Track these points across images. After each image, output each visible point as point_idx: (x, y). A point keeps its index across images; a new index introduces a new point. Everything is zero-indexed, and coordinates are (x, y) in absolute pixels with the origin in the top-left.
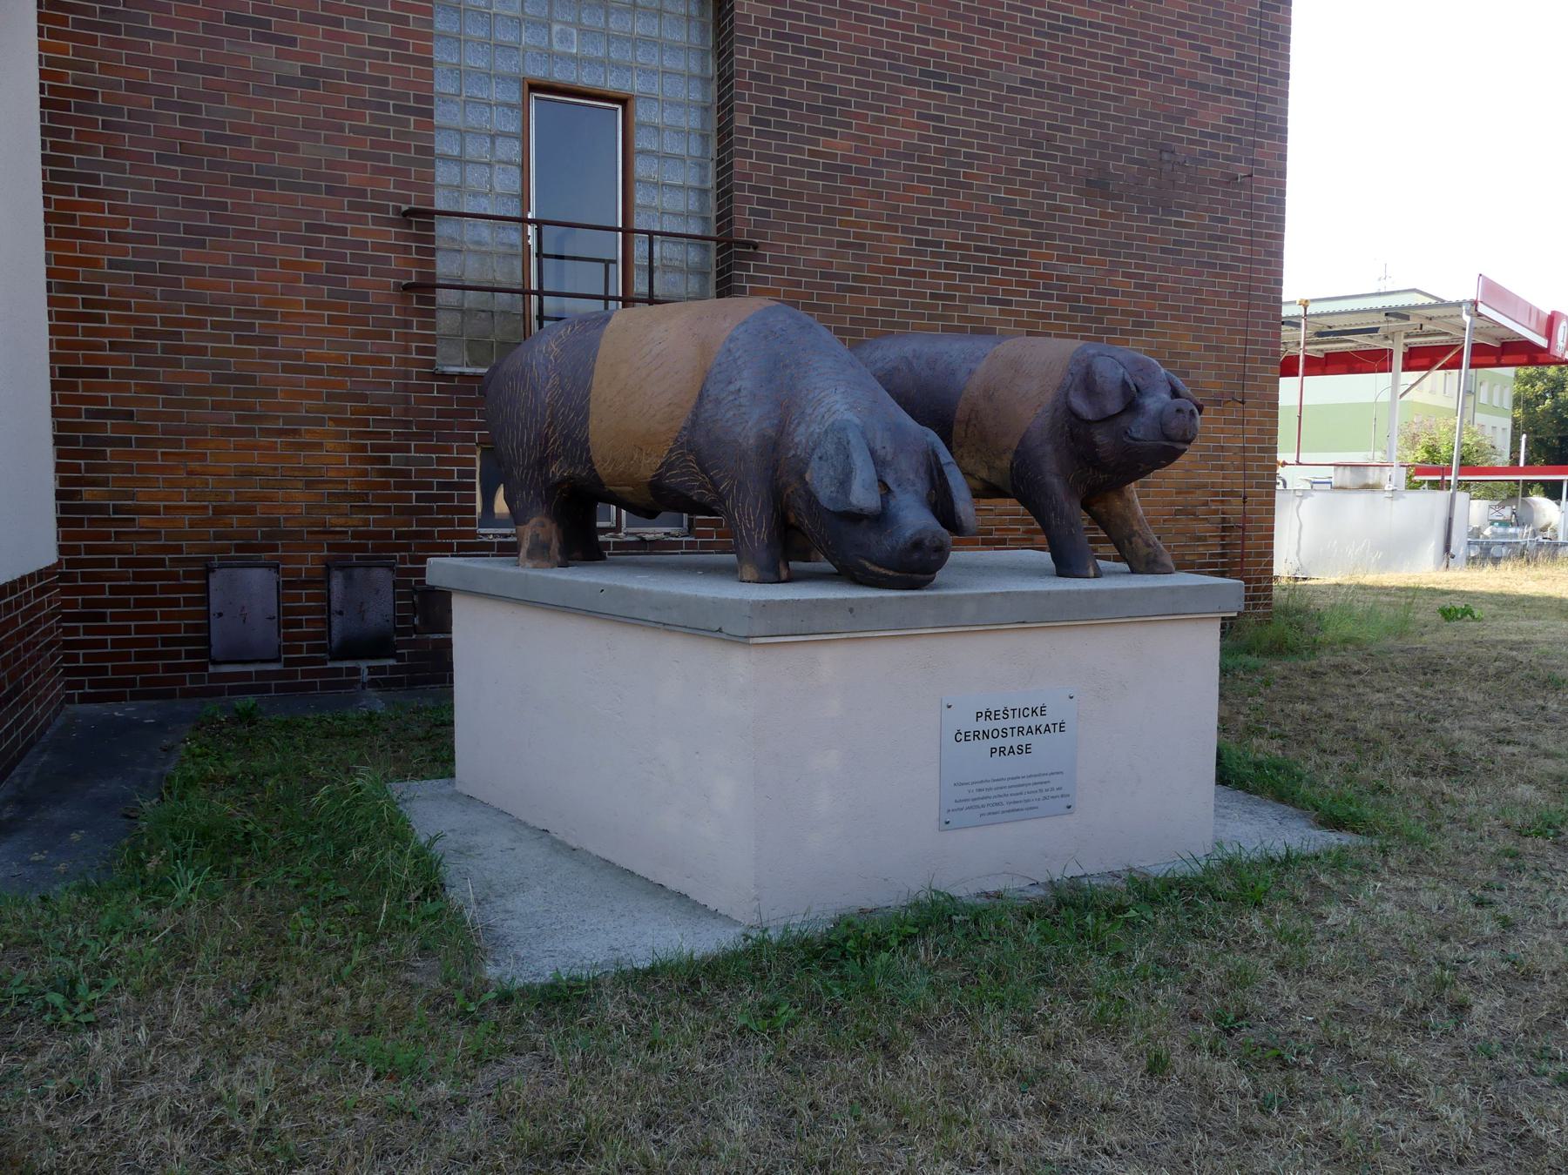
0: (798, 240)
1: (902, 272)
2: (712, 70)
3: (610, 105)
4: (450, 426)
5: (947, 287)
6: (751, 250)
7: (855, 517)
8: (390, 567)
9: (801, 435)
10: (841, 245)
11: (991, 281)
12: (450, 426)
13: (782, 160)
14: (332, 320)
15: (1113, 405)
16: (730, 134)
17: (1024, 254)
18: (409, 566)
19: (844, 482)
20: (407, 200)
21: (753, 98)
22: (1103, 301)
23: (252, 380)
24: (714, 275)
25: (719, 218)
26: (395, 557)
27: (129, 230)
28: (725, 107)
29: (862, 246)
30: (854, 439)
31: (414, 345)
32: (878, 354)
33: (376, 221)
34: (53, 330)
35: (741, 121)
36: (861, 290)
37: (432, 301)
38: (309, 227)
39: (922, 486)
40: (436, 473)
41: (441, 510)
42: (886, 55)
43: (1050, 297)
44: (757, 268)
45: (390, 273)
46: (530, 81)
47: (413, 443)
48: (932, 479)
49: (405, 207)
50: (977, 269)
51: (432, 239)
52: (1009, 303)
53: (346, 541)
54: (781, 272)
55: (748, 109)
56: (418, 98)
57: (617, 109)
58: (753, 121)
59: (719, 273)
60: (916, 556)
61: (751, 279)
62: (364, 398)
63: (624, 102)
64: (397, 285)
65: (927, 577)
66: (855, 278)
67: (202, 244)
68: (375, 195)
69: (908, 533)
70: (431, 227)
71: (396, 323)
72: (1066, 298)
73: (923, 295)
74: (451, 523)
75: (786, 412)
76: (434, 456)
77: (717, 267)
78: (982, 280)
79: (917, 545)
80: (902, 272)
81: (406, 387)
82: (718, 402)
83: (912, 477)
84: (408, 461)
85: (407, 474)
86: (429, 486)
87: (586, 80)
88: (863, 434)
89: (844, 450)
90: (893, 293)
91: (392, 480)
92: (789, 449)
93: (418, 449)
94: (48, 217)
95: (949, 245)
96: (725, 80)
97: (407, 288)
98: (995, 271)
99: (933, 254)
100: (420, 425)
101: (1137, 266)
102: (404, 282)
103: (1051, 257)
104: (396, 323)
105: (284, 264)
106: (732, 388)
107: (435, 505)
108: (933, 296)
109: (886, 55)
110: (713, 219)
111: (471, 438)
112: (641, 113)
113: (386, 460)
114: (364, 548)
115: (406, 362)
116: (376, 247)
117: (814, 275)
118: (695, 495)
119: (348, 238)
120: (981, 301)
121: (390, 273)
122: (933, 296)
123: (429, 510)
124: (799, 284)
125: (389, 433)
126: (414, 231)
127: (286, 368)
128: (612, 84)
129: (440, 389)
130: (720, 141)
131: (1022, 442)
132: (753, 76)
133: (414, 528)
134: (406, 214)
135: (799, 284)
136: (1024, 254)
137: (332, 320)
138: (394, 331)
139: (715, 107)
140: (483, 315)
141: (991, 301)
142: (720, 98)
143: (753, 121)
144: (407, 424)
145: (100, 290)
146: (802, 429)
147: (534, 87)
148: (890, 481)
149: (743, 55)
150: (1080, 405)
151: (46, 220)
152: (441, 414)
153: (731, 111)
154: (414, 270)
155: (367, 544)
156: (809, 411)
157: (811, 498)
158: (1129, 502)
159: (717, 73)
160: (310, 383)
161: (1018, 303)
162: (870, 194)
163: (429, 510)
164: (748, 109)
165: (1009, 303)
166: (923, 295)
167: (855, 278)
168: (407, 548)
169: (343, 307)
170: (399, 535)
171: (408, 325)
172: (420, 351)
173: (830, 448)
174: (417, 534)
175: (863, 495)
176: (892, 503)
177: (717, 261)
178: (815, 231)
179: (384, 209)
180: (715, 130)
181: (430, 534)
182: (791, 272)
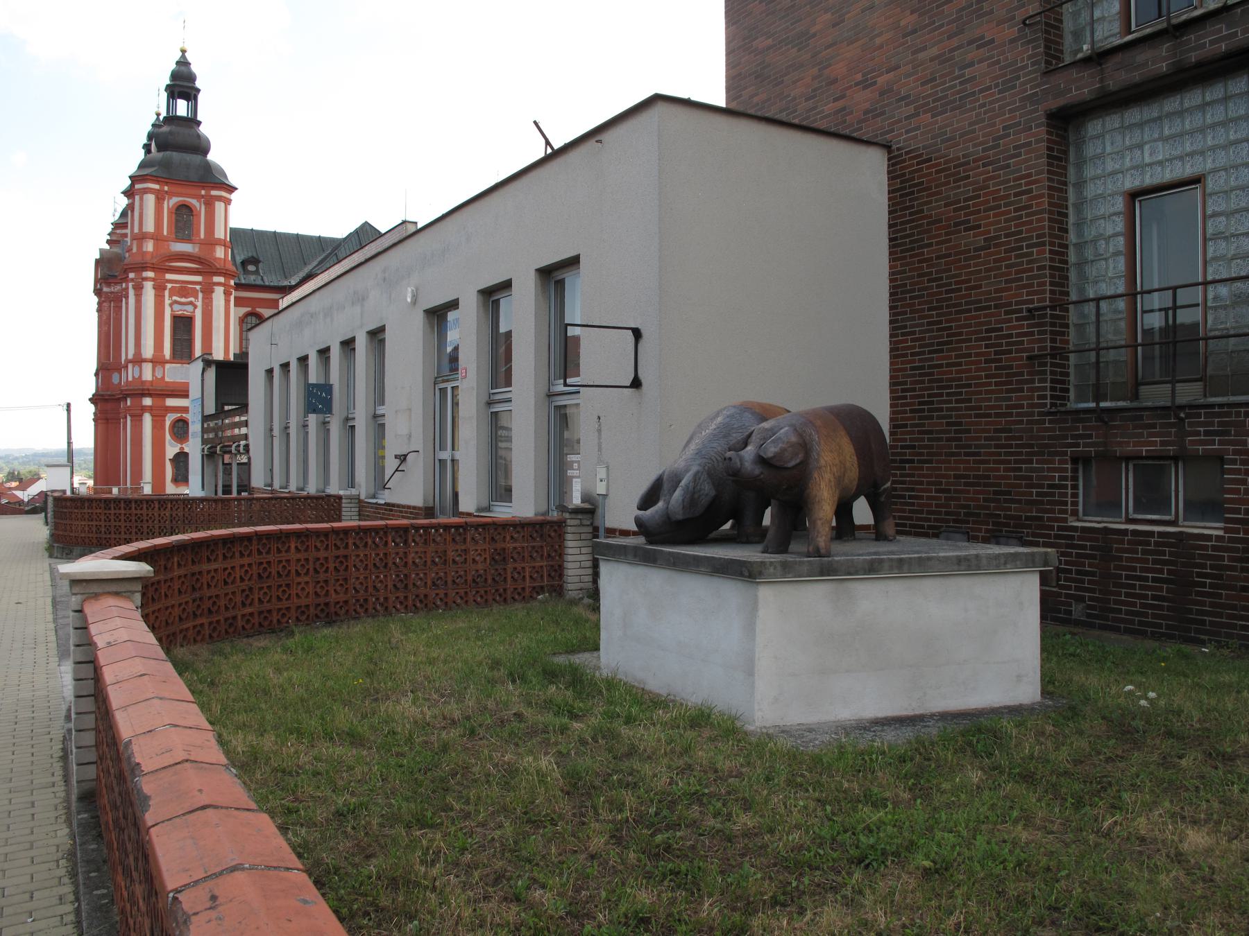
3: (1194, 186)
14: (997, 384)
26: (1023, 532)
27: (917, 350)
34: (892, 406)
40: (1046, 478)
41: (1049, 503)
63: (1196, 180)
71: (1027, 382)
74: (1053, 511)
84: (1032, 470)
85: (1031, 478)
87: (1168, 175)
91: (1024, 482)
94: (891, 350)
104: (1027, 382)
111: (1065, 453)
112: (1210, 184)
114: (1007, 525)
123: (1042, 502)
129: (1051, 422)
137: (997, 384)
144: (1031, 446)
145: (906, 383)
168: (1029, 527)
170: (1027, 518)
181: (1041, 519)
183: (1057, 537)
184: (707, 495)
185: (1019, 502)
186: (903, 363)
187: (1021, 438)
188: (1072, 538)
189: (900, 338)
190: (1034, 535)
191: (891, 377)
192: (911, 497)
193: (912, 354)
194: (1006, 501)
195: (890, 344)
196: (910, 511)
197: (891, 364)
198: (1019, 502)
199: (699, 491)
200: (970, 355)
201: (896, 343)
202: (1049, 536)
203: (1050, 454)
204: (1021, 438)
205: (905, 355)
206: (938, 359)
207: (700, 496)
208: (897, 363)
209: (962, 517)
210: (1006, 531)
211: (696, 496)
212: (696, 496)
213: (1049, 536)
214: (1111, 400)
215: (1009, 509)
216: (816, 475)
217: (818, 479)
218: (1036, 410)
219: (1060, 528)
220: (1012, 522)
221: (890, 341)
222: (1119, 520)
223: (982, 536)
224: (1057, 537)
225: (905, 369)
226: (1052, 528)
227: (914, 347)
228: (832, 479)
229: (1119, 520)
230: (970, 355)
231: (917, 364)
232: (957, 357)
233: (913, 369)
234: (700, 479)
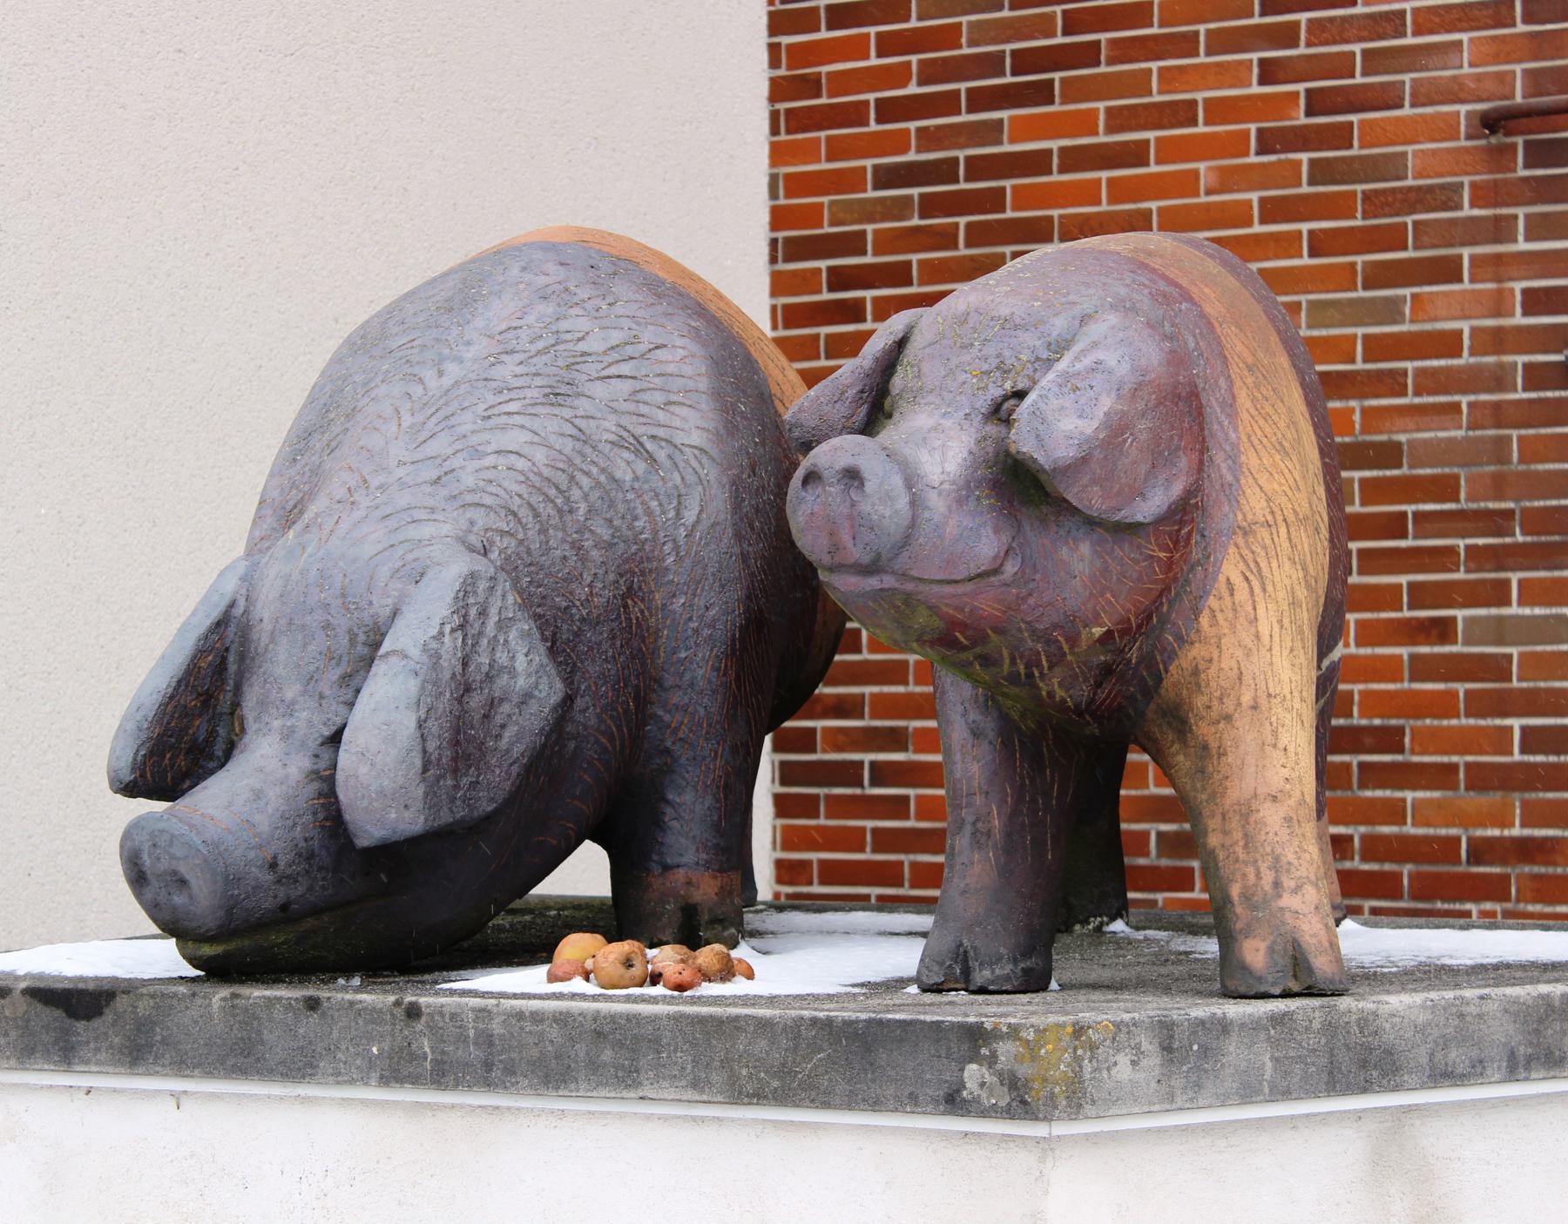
14: (1319, 245)
27: (913, 89)
31: (1518, 286)
45: (1453, 92)
67: (1042, 93)
71: (1472, 232)
81: (1499, 415)
84: (1501, 631)
85: (1498, 668)
91: (1461, 688)
94: (778, 90)
97: (1491, 123)
104: (1472, 232)
113: (1442, 630)
121: (1453, 92)
125: (1451, 551)
137: (1319, 245)
144: (1497, 522)
145: (854, 244)
151: (774, 97)
154: (1518, 68)
155: (1398, 876)
170: (1482, 851)
174: (1526, 850)
184: (527, 697)
185: (1442, 776)
186: (837, 150)
187: (1445, 488)
189: (824, 34)
191: (779, 218)
192: (882, 774)
193: (887, 110)
195: (774, 63)
196: (884, 840)
197: (778, 154)
198: (1442, 776)
199: (489, 678)
200: (1184, 113)
201: (800, 55)
205: (856, 114)
206: (1024, 130)
207: (492, 704)
208: (808, 152)
211: (476, 701)
212: (476, 701)
215: (1395, 812)
216: (1231, 569)
217: (1242, 594)
218: (1521, 359)
220: (1407, 869)
221: (774, 49)
225: (852, 180)
227: (899, 76)
228: (1301, 593)
230: (1184, 113)
231: (912, 156)
232: (1118, 121)
233: (887, 177)
234: (483, 613)
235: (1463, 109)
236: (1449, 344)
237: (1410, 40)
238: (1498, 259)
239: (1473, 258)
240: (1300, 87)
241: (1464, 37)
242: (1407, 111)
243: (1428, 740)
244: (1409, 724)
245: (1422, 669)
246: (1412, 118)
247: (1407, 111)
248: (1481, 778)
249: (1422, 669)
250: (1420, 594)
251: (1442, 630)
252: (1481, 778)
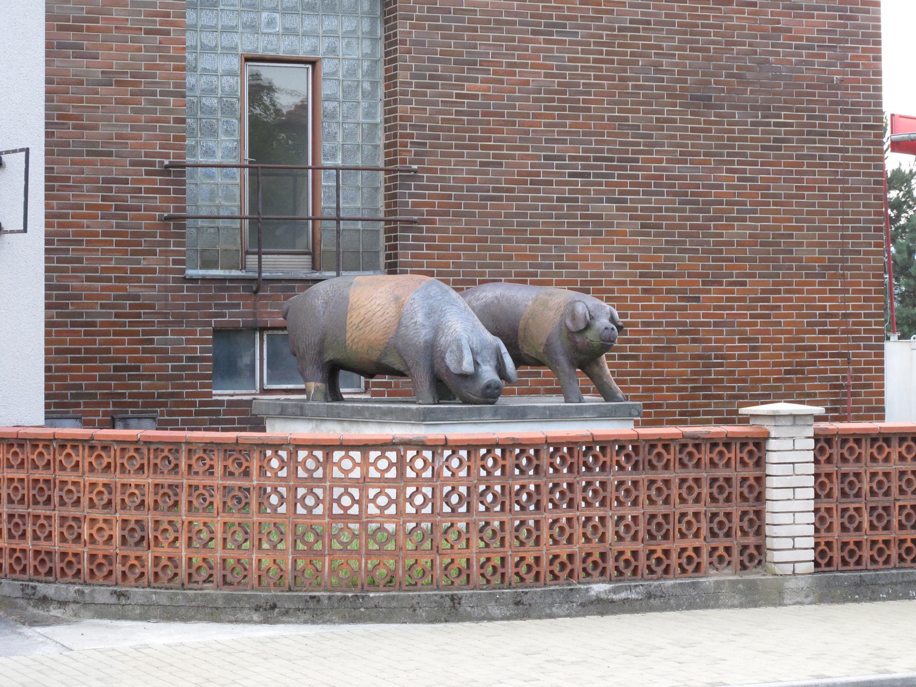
0: (449, 163)
1: (532, 183)
2: (380, 32)
4: (195, 316)
5: (570, 192)
6: (412, 173)
7: (465, 376)
8: (154, 418)
9: (443, 341)
10: (483, 164)
11: (607, 184)
12: (195, 316)
13: (436, 103)
14: (118, 243)
15: (582, 326)
16: (395, 85)
17: (637, 160)
18: (166, 418)
19: (460, 361)
20: (167, 156)
21: (413, 59)
22: (708, 195)
23: (66, 288)
24: (382, 190)
25: (387, 146)
26: (156, 412)
28: (391, 60)
29: (500, 165)
30: (464, 342)
31: (171, 258)
32: (484, 294)
33: (148, 173)
35: (403, 76)
36: (500, 199)
37: (183, 227)
38: (105, 181)
39: (493, 363)
40: (185, 350)
41: (189, 377)
42: (516, 15)
43: (662, 194)
44: (417, 187)
45: (156, 209)
46: (246, 56)
47: (169, 329)
48: (498, 359)
49: (166, 162)
50: (596, 175)
51: (183, 183)
52: (625, 201)
53: (125, 400)
54: (436, 188)
55: (409, 68)
56: (176, 85)
57: (308, 68)
58: (413, 77)
59: (387, 189)
60: (489, 391)
61: (412, 196)
62: (137, 297)
64: (161, 217)
65: (493, 400)
66: (495, 190)
68: (147, 155)
69: (485, 381)
70: (183, 174)
71: (160, 244)
72: (675, 194)
73: (551, 200)
74: (194, 386)
75: (437, 330)
76: (184, 337)
77: (385, 183)
78: (600, 184)
79: (488, 386)
80: (532, 183)
81: (166, 289)
82: (407, 327)
83: (488, 359)
84: (166, 342)
85: (165, 351)
86: (180, 359)
88: (468, 342)
89: (460, 349)
90: (526, 199)
91: (155, 356)
92: (437, 347)
93: (173, 333)
95: (572, 158)
96: (390, 40)
97: (167, 219)
98: (612, 176)
99: (558, 167)
100: (174, 315)
101: (739, 163)
102: (166, 214)
103: (661, 161)
104: (160, 244)
105: (89, 207)
106: (413, 321)
107: (184, 373)
108: (559, 200)
109: (516, 15)
110: (382, 146)
111: (209, 324)
113: (151, 341)
114: (135, 405)
115: (165, 271)
116: (148, 191)
117: (461, 189)
118: (396, 367)
119: (129, 186)
120: (601, 201)
122: (559, 200)
123: (180, 377)
124: (449, 197)
125: (154, 322)
126: (172, 178)
127: (88, 279)
128: (303, 49)
130: (387, 87)
131: (548, 340)
132: (414, 43)
133: (170, 390)
134: (166, 167)
135: (449, 197)
136: (637, 160)
137: (118, 243)
138: (158, 249)
139: (382, 60)
140: (212, 230)
141: (609, 201)
142: (387, 54)
143: (413, 77)
144: (166, 315)
146: (443, 339)
147: (248, 59)
148: (479, 360)
149: (403, 28)
150: (569, 323)
152: (189, 307)
153: (395, 68)
154: (172, 205)
155: (138, 402)
156: (446, 331)
157: (447, 368)
158: (602, 368)
159: (384, 35)
160: (103, 289)
161: (632, 201)
162: (506, 123)
163: (180, 377)
164: (409, 68)
165: (625, 201)
166: (551, 200)
167: (495, 190)
168: (164, 405)
169: (124, 234)
170: (160, 395)
171: (167, 244)
172: (175, 262)
173: (455, 348)
174: (172, 395)
175: (467, 366)
176: (480, 370)
177: (385, 178)
178: (462, 155)
179: (153, 164)
180: (383, 77)
181: (179, 395)
182: (443, 188)
183: (198, 413)
185: (151, 377)
187: (152, 307)
188: (217, 413)
190: (170, 413)
194: (131, 377)
202: (189, 413)
203: (189, 324)
204: (152, 307)
209: (69, 400)
210: (132, 412)
213: (189, 413)
214: (222, 268)
218: (171, 276)
219: (202, 404)
220: (140, 401)
222: (253, 391)
223: (99, 420)
224: (198, 413)
226: (193, 404)
229: (253, 391)
235: (157, 213)
236: (153, 271)
237: (143, 195)
238: (166, 251)
239: (160, 250)
240: (113, 203)
241: (158, 196)
242: (142, 212)
243: (145, 369)
244: (141, 365)
245: (145, 351)
246: (144, 214)
247: (142, 212)
248: (160, 378)
249: (145, 351)
250: (145, 333)
251: (151, 341)
252: (160, 378)
